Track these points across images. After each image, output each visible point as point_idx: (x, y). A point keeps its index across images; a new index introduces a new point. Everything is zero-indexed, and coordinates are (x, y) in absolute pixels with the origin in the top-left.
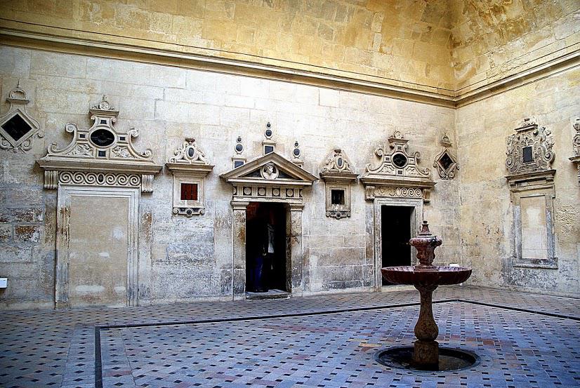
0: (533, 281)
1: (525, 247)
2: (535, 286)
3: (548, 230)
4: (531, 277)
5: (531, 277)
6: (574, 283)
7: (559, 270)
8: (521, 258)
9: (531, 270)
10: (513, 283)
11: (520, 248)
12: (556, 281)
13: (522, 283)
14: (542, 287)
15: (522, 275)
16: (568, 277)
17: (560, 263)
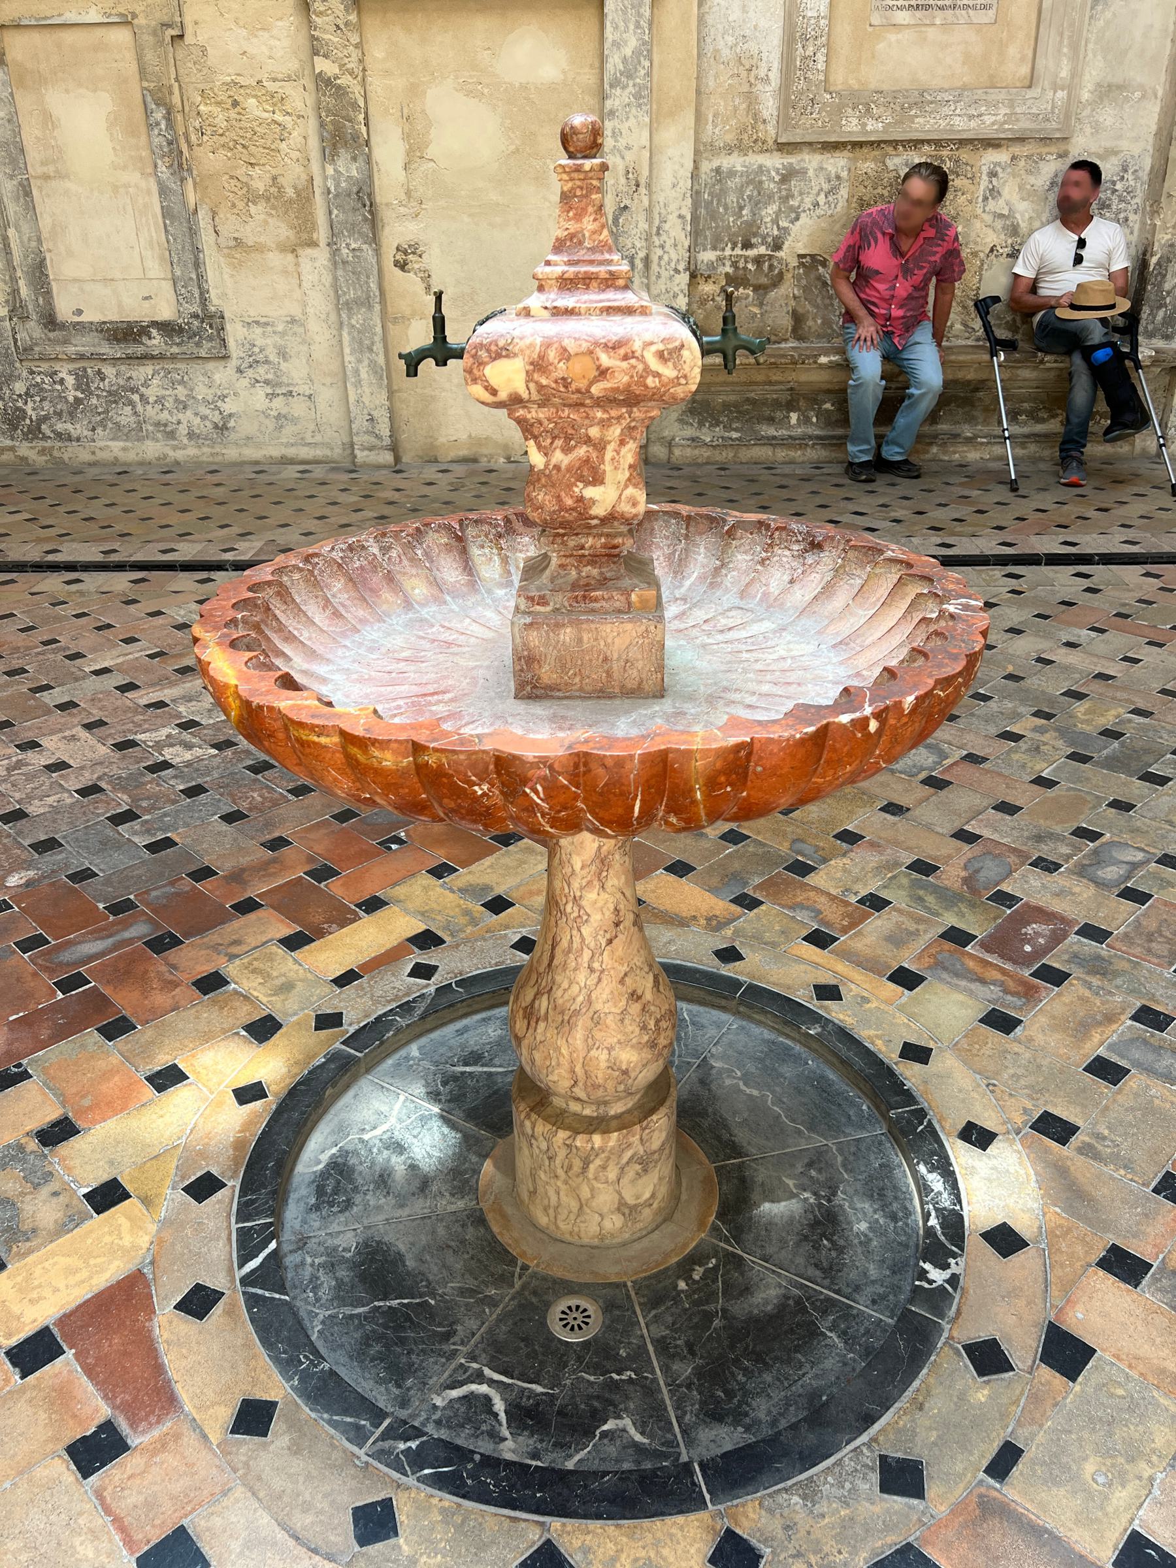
0: (125, 416)
1: (61, 269)
2: (137, 432)
3: (163, 191)
4: (114, 397)
5: (114, 397)
6: (298, 408)
7: (234, 363)
8: (50, 321)
9: (109, 371)
10: (34, 432)
11: (39, 273)
12: (228, 407)
13: (78, 429)
14: (171, 435)
15: (71, 395)
16: (277, 387)
17: (235, 333)
